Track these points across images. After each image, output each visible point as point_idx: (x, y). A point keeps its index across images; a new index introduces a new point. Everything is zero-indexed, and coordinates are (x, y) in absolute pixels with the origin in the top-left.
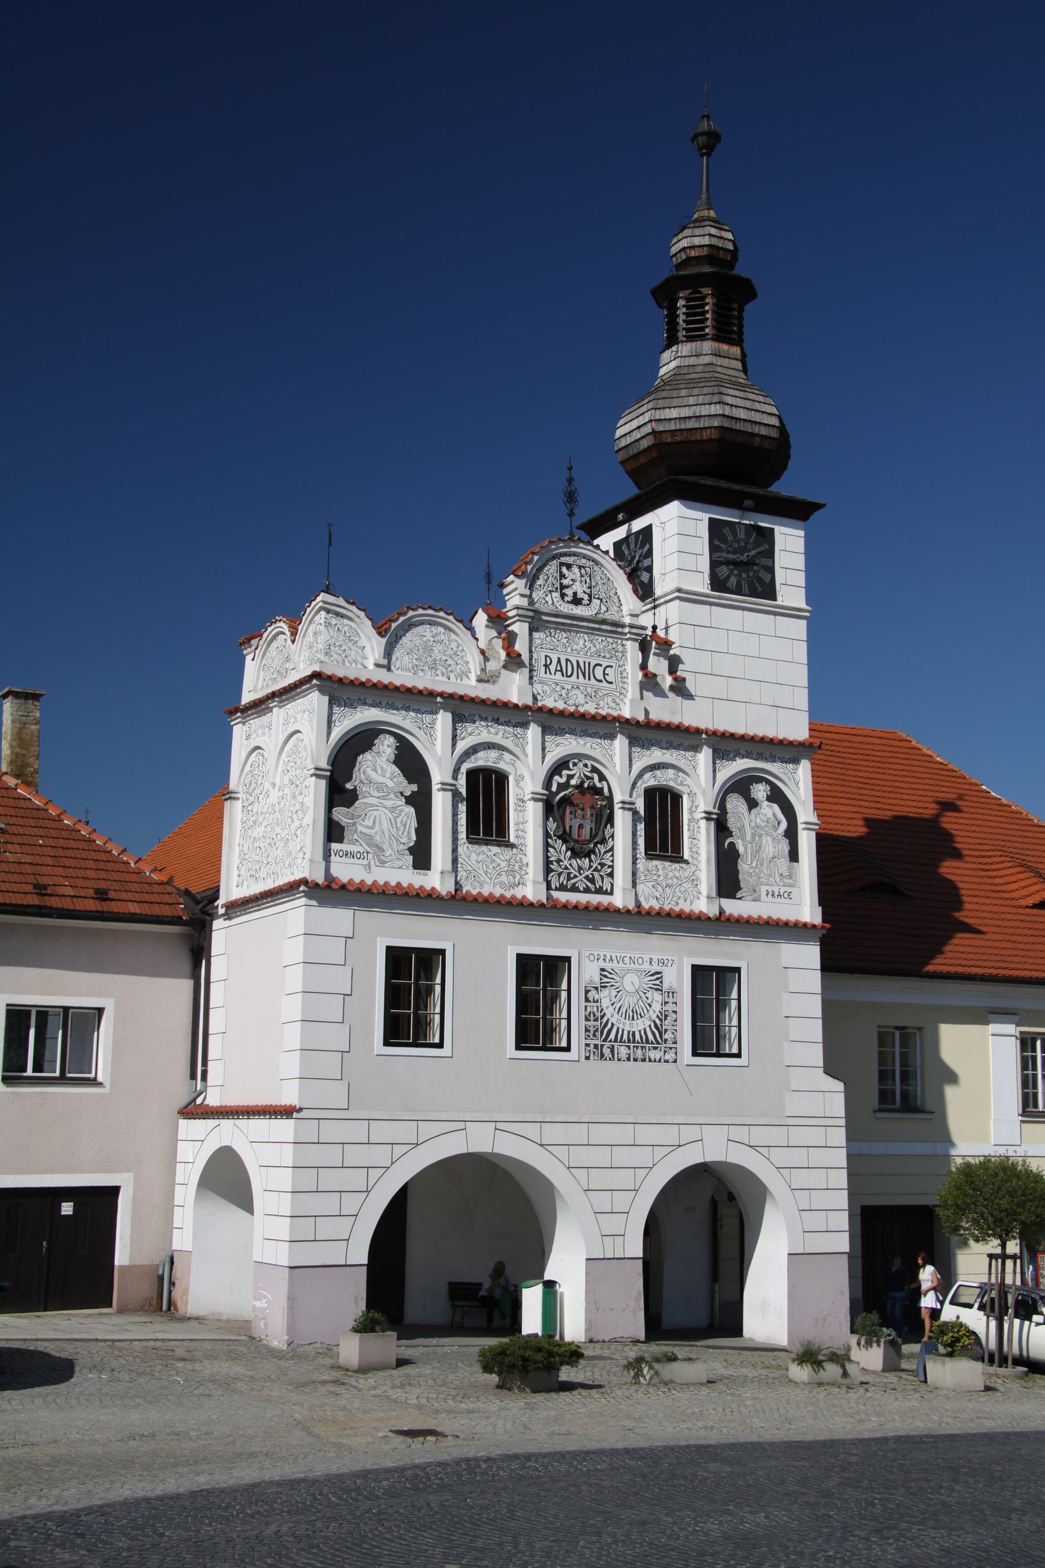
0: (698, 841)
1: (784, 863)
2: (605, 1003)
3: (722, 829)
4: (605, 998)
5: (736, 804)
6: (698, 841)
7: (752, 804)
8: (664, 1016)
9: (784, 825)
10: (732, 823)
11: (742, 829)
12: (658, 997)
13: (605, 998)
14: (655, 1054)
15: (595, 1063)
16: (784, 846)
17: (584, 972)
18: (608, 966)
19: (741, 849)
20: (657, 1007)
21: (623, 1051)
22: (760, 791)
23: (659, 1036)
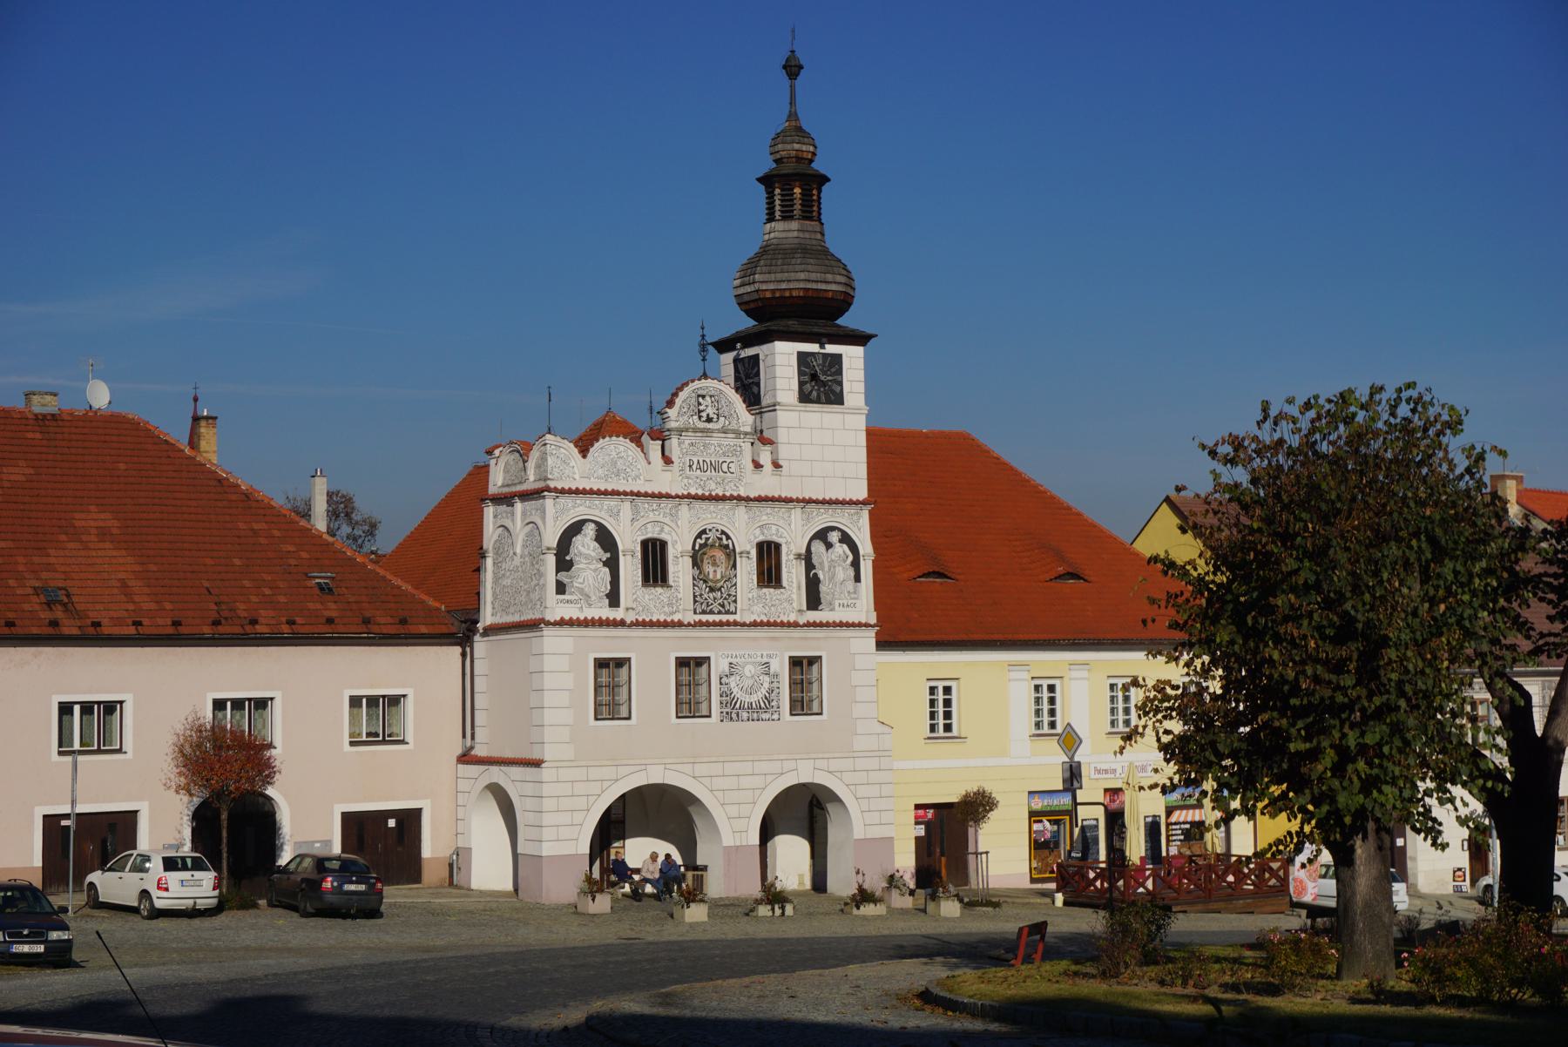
0: (793, 574)
1: (850, 584)
2: (733, 685)
3: (810, 566)
4: (733, 681)
5: (818, 547)
6: (793, 574)
7: (829, 546)
8: (771, 691)
9: (851, 558)
10: (815, 560)
11: (822, 563)
12: (767, 679)
13: (733, 681)
14: (765, 716)
15: (727, 724)
16: (851, 573)
17: (719, 666)
18: (734, 661)
19: (821, 576)
20: (766, 685)
21: (745, 715)
22: (834, 537)
23: (768, 703)
